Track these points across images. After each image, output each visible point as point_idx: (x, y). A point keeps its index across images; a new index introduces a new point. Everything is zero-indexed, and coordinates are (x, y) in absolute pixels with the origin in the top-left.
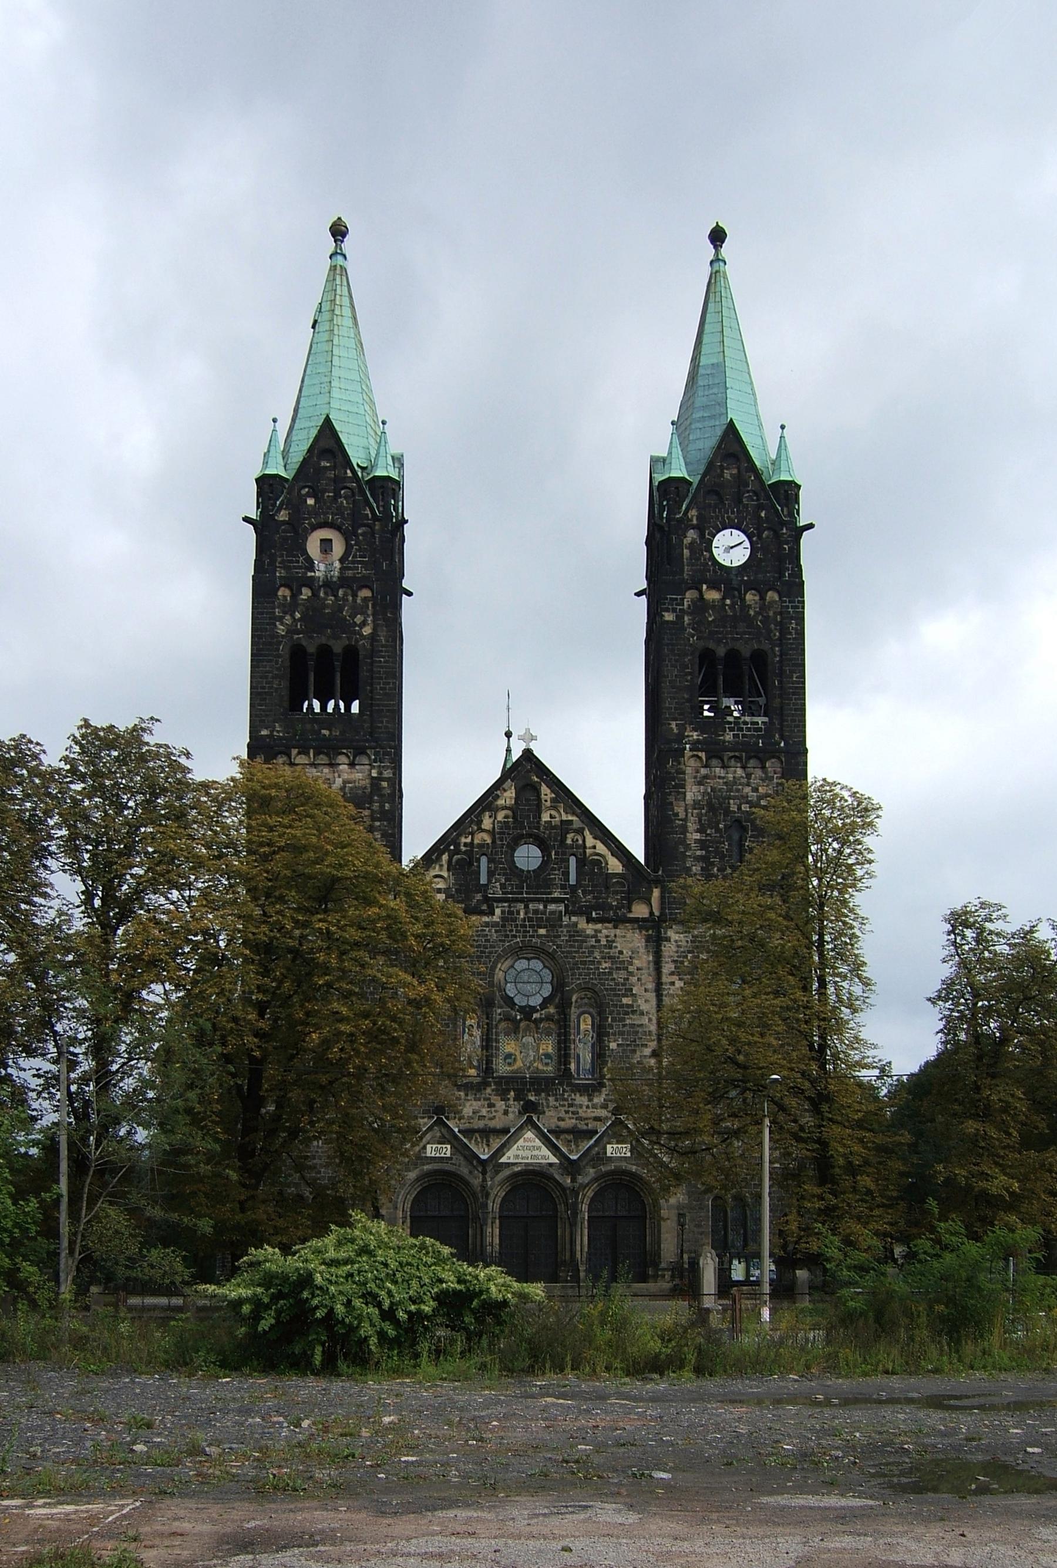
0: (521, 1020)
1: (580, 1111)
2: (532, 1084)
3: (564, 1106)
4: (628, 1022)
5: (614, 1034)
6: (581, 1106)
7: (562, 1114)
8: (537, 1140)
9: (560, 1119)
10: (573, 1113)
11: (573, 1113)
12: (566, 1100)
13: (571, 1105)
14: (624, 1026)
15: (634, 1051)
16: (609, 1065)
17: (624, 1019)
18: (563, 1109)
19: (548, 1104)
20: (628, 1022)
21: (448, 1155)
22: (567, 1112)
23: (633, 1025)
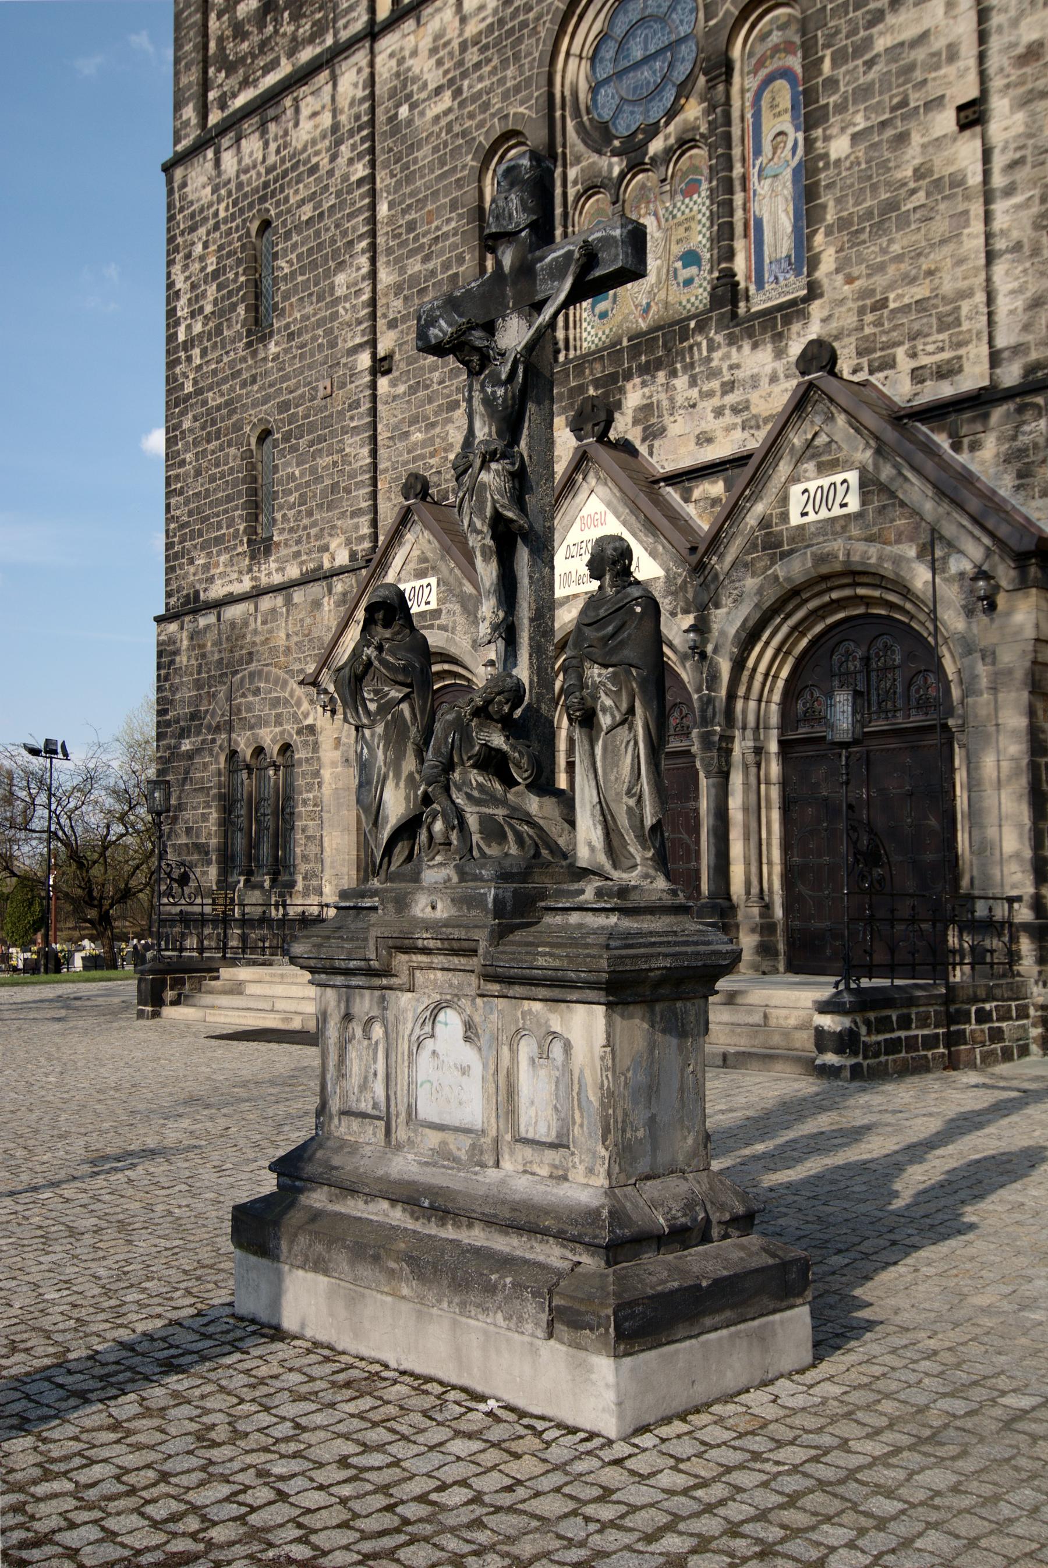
0: (622, 175)
1: (754, 397)
2: (635, 351)
3: (710, 394)
4: (881, 44)
5: (841, 108)
6: (754, 381)
7: (710, 423)
8: (611, 518)
9: (705, 439)
10: (735, 410)
11: (735, 410)
12: (714, 374)
13: (729, 387)
14: (870, 64)
15: (902, 138)
16: (830, 217)
17: (868, 42)
18: (707, 406)
19: (672, 400)
20: (881, 44)
21: (433, 606)
22: (719, 412)
23: (895, 51)
